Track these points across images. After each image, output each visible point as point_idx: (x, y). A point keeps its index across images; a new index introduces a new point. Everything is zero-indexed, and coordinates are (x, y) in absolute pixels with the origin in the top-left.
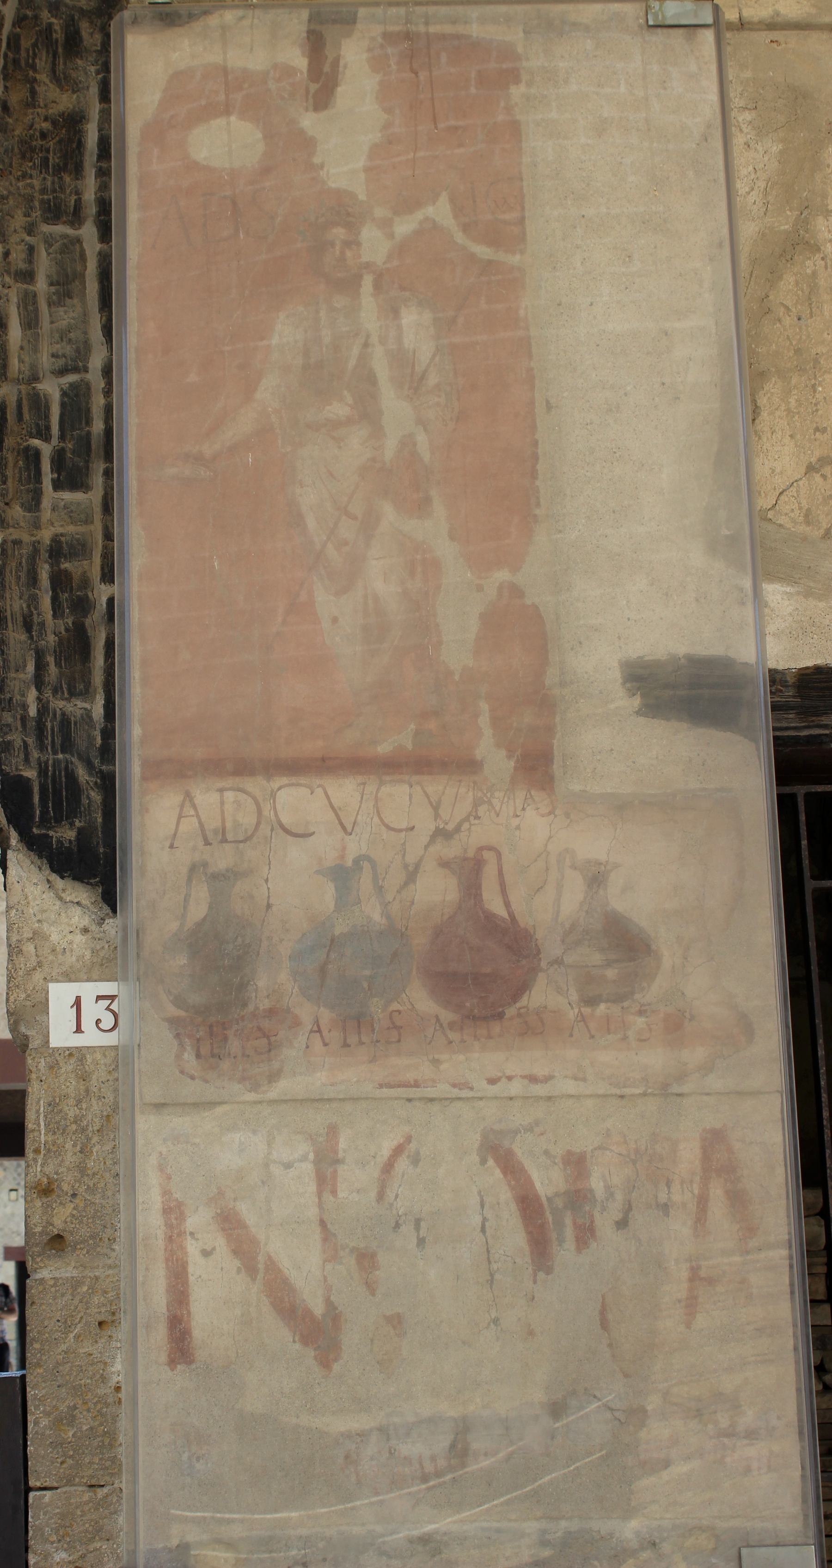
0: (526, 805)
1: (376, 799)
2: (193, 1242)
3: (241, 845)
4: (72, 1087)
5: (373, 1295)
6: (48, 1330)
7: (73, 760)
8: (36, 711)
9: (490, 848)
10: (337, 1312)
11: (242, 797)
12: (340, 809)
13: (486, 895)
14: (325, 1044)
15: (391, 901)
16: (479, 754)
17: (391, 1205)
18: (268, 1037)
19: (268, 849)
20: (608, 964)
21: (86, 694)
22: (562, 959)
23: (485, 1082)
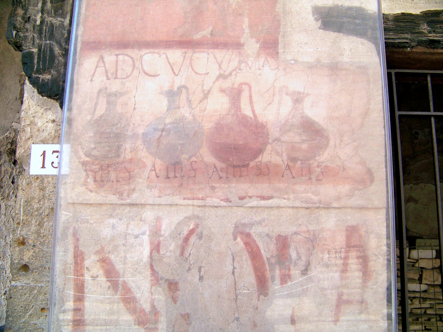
0: (264, 64)
1: (191, 59)
2: (88, 272)
3: (124, 80)
4: (37, 194)
5: (175, 303)
6: (16, 311)
7: (53, 43)
8: (39, 22)
9: (246, 84)
10: (157, 311)
11: (127, 58)
12: (173, 64)
13: (242, 106)
15: (195, 107)
16: (242, 41)
17: (187, 259)
19: (137, 82)
20: (303, 141)
21: (62, 14)
22: (280, 139)
23: (238, 199)
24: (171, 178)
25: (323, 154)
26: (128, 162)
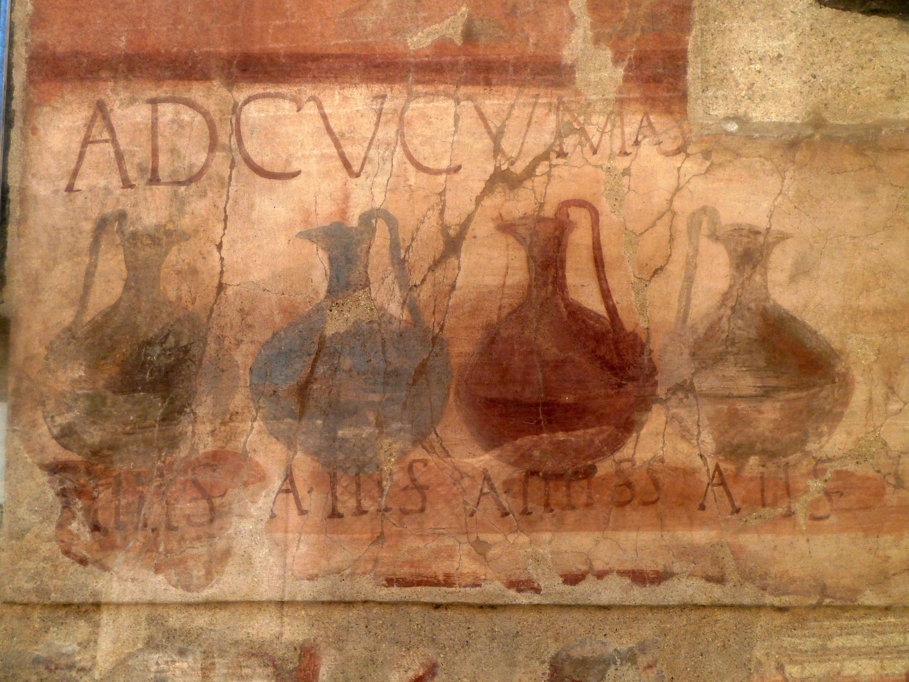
9: (581, 204)
11: (187, 114)
12: (343, 135)
13: (571, 278)
14: (302, 512)
15: (418, 283)
16: (567, 55)
18: (209, 499)
19: (225, 197)
22: (692, 384)
23: (561, 580)
24: (348, 518)
25: (830, 433)
26: (207, 465)
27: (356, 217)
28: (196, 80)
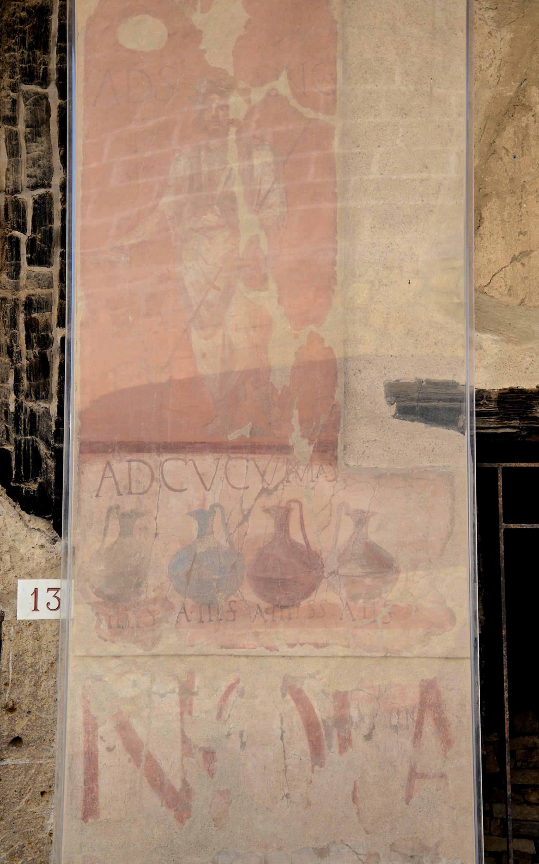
9: (296, 501)
11: (142, 465)
12: (203, 474)
21: (46, 398)
27: (209, 507)
28: (146, 452)
